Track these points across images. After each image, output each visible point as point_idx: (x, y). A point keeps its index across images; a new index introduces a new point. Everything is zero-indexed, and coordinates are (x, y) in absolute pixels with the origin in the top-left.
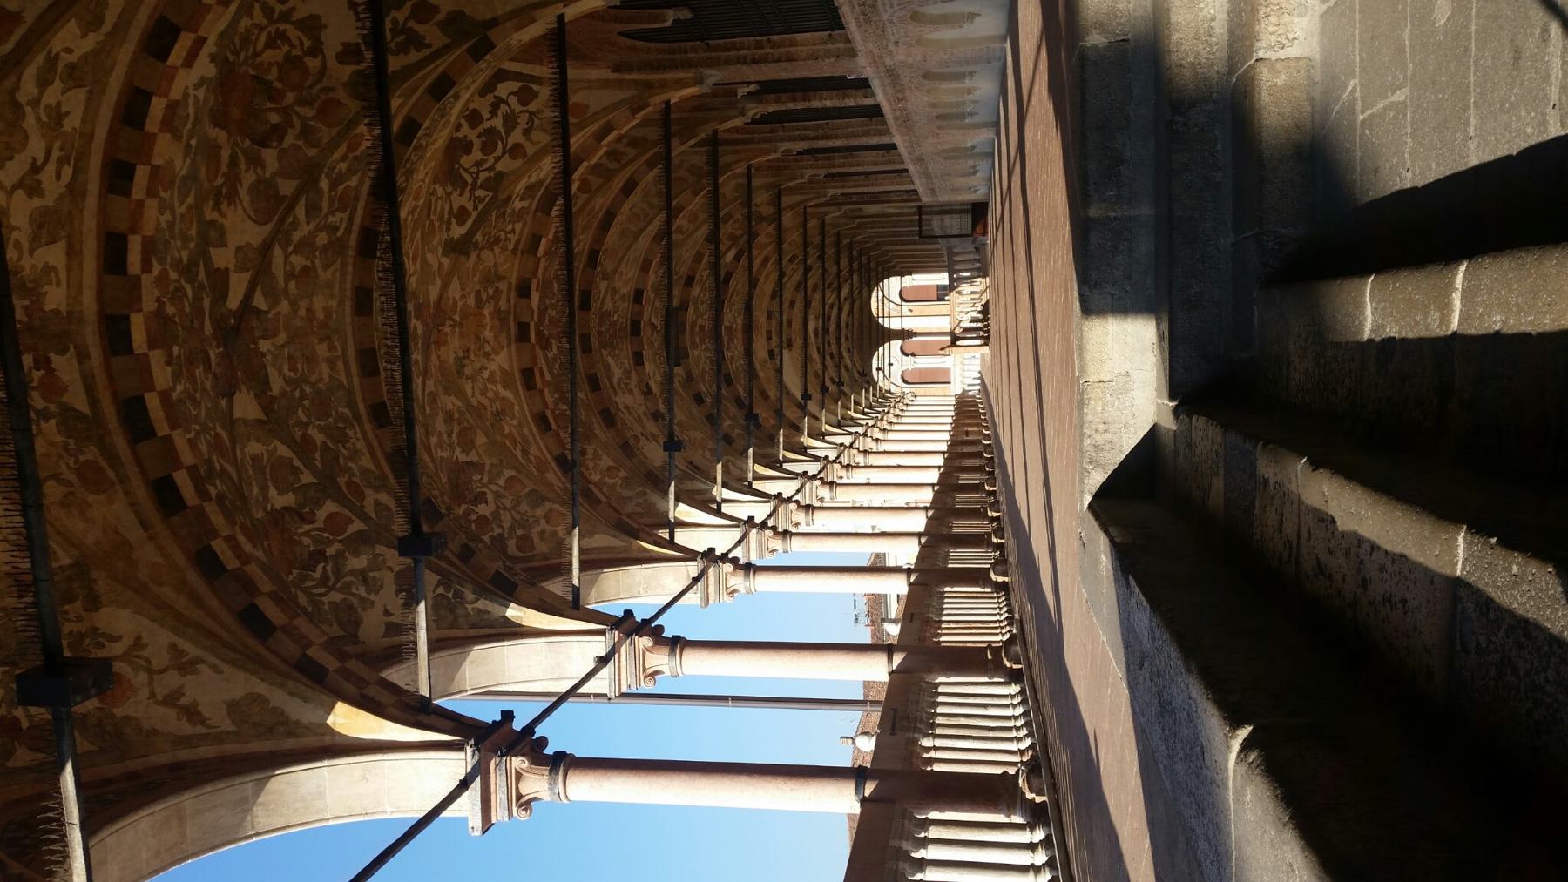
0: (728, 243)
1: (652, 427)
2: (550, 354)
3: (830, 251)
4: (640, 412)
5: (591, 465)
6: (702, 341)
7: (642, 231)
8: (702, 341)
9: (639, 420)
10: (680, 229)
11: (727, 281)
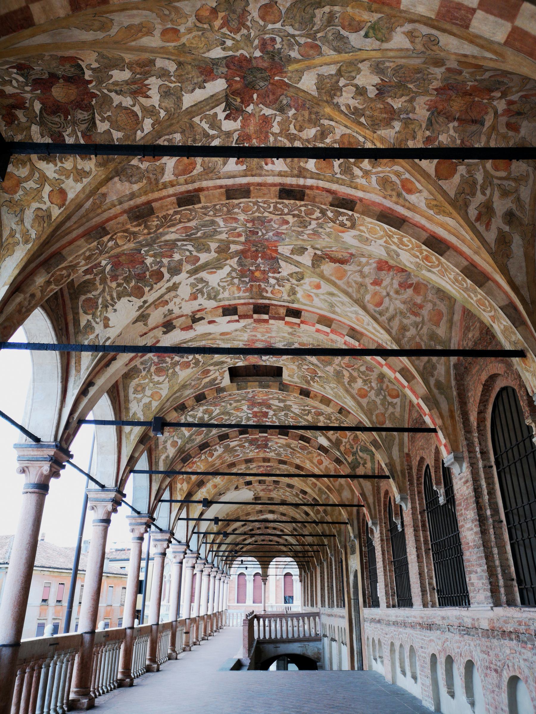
0: (334, 438)
1: (156, 317)
2: (220, 111)
3: (319, 529)
4: (171, 306)
5: (68, 164)
6: (255, 414)
7: (364, 308)
8: (255, 414)
9: (161, 302)
10: (352, 379)
11: (302, 438)
